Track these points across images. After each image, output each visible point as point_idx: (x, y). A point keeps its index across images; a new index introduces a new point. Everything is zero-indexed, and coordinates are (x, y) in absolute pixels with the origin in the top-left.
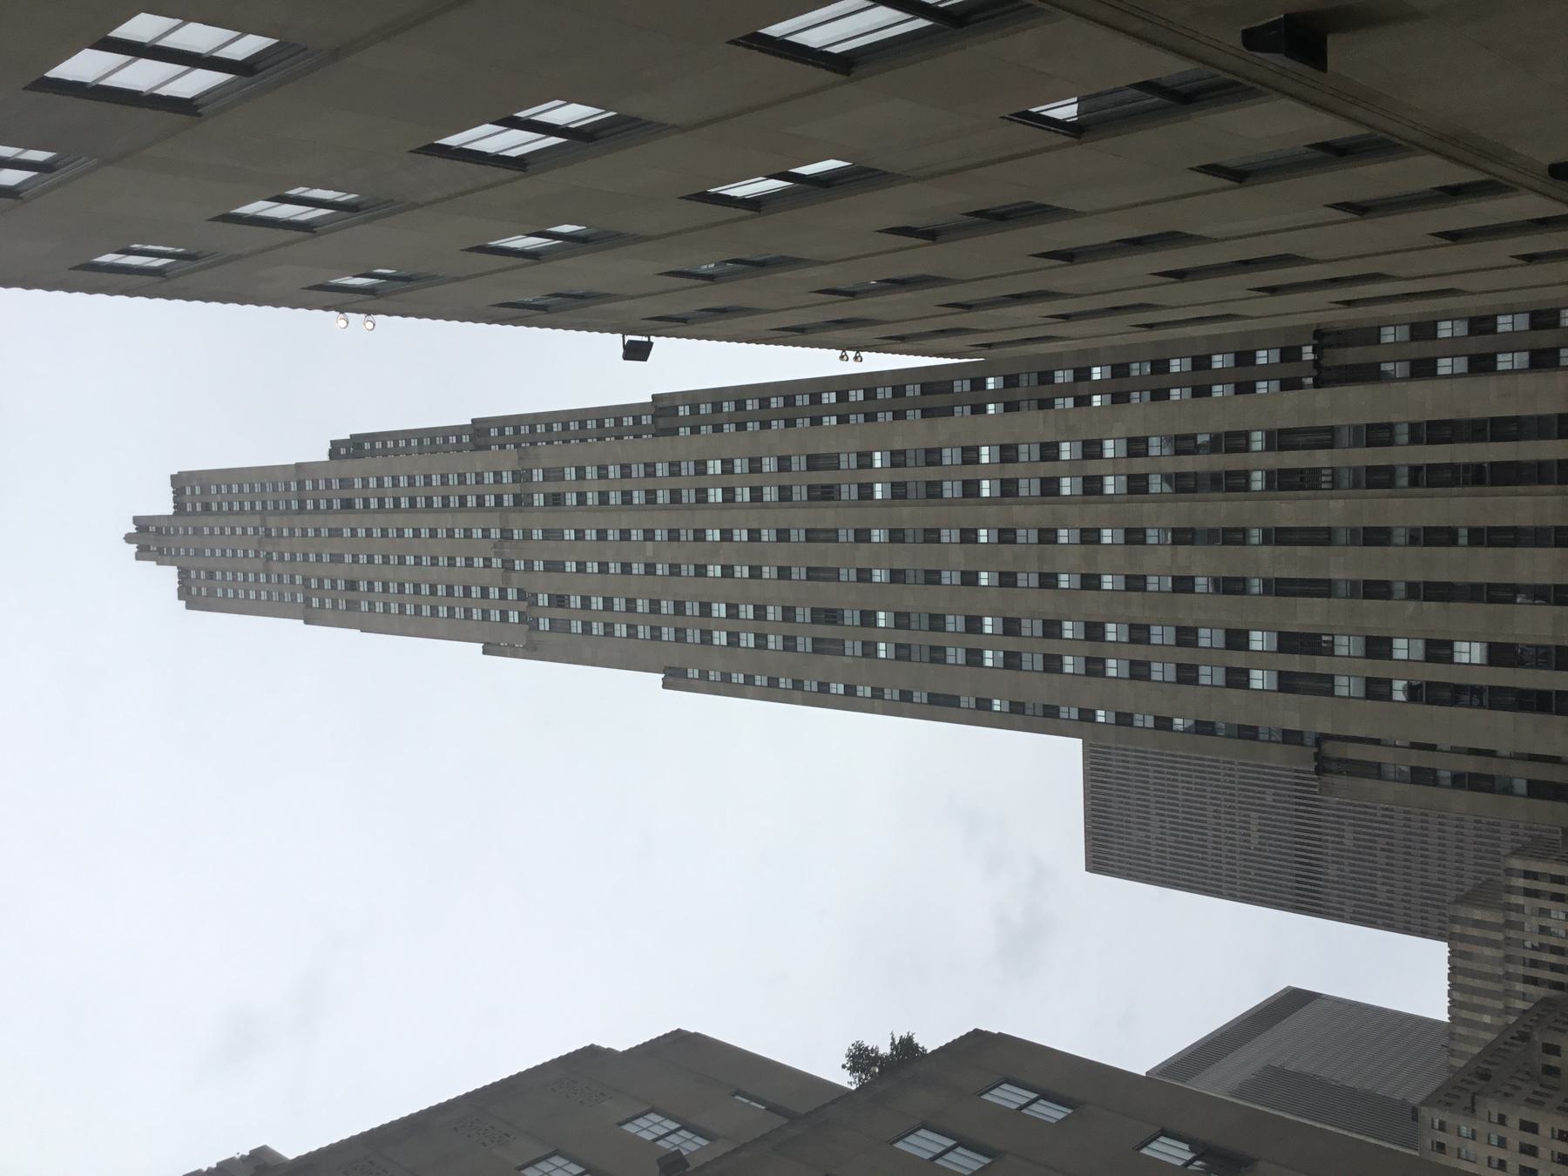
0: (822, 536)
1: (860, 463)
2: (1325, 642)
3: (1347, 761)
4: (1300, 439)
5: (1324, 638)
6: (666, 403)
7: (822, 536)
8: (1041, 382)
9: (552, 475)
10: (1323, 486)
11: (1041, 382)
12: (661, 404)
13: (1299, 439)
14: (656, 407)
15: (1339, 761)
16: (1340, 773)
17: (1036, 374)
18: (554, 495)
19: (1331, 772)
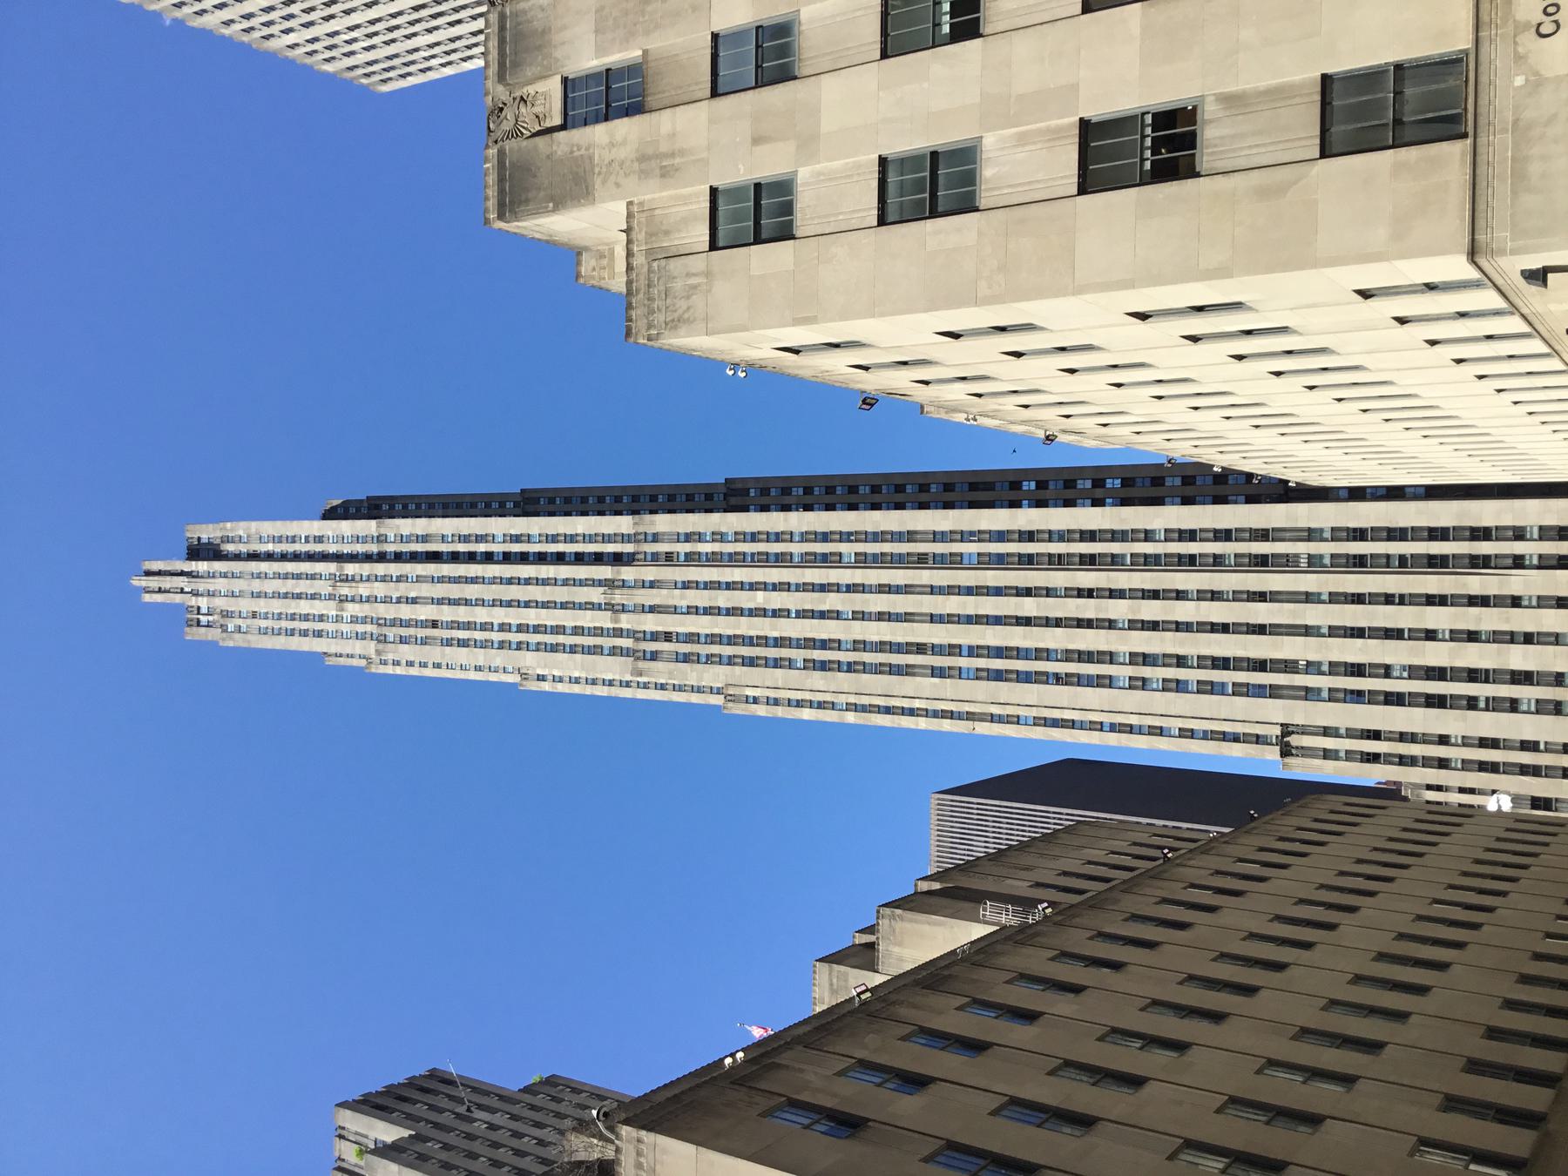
0: (918, 589)
1: (952, 538)
2: (1302, 665)
3: (1302, 748)
4: (1288, 535)
5: (1301, 662)
6: (739, 486)
7: (918, 589)
8: (1066, 487)
9: (665, 537)
10: (1302, 565)
11: (1066, 487)
12: (733, 486)
13: (1288, 535)
14: (728, 488)
15: (1297, 748)
16: (1298, 756)
17: (1062, 482)
18: (666, 553)
19: (1292, 755)
